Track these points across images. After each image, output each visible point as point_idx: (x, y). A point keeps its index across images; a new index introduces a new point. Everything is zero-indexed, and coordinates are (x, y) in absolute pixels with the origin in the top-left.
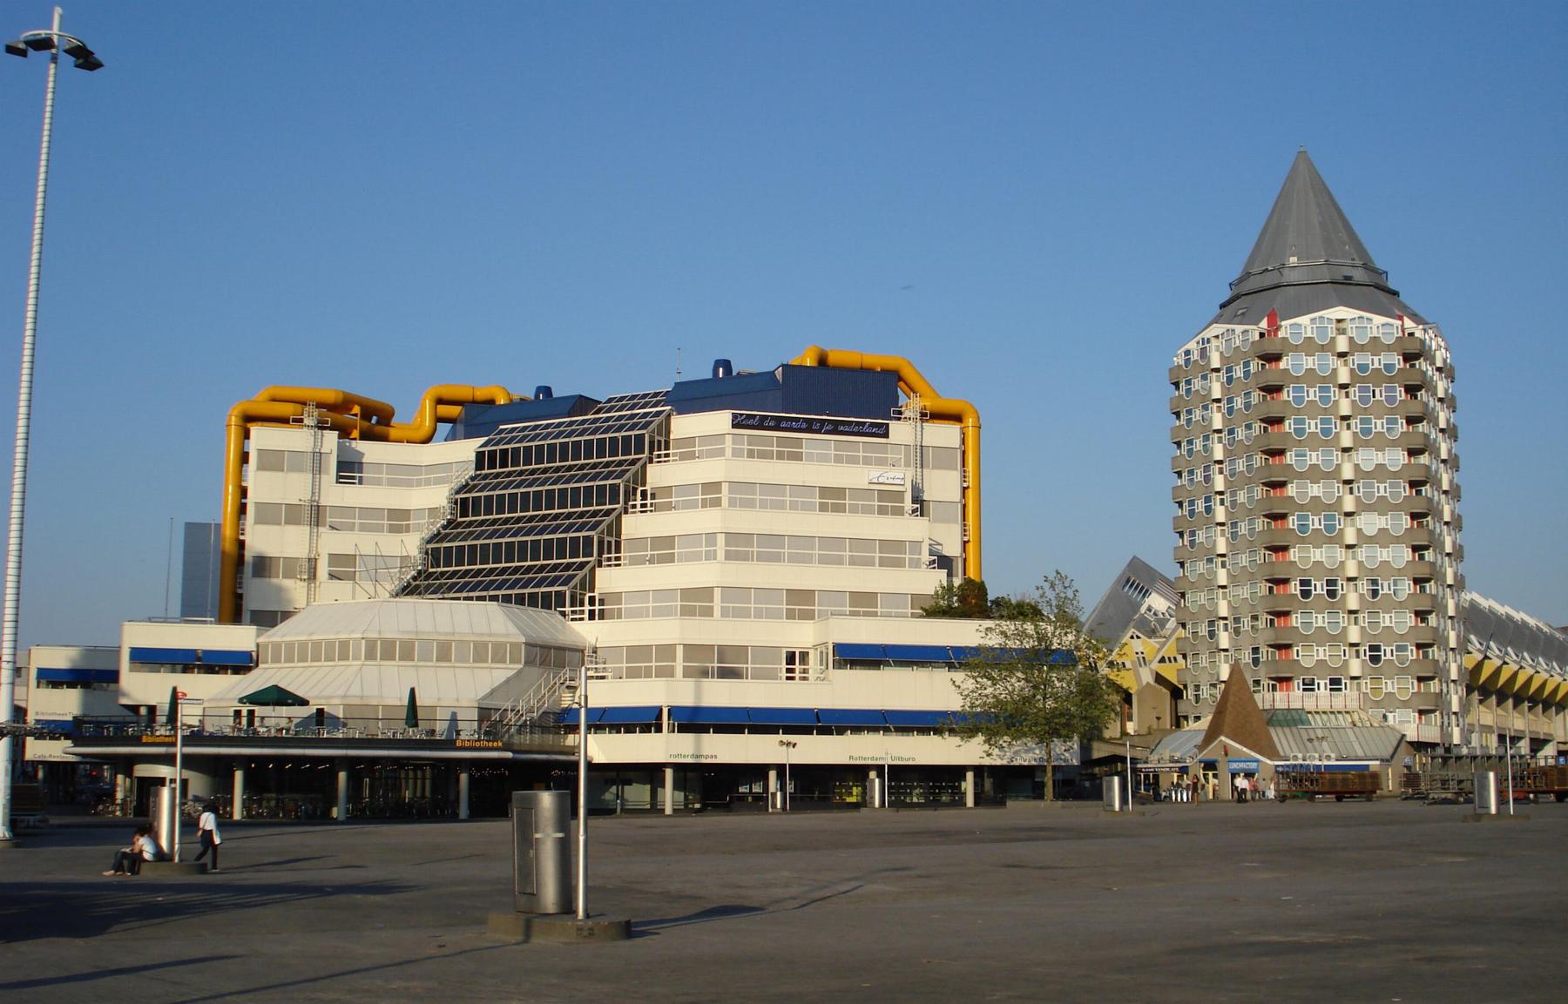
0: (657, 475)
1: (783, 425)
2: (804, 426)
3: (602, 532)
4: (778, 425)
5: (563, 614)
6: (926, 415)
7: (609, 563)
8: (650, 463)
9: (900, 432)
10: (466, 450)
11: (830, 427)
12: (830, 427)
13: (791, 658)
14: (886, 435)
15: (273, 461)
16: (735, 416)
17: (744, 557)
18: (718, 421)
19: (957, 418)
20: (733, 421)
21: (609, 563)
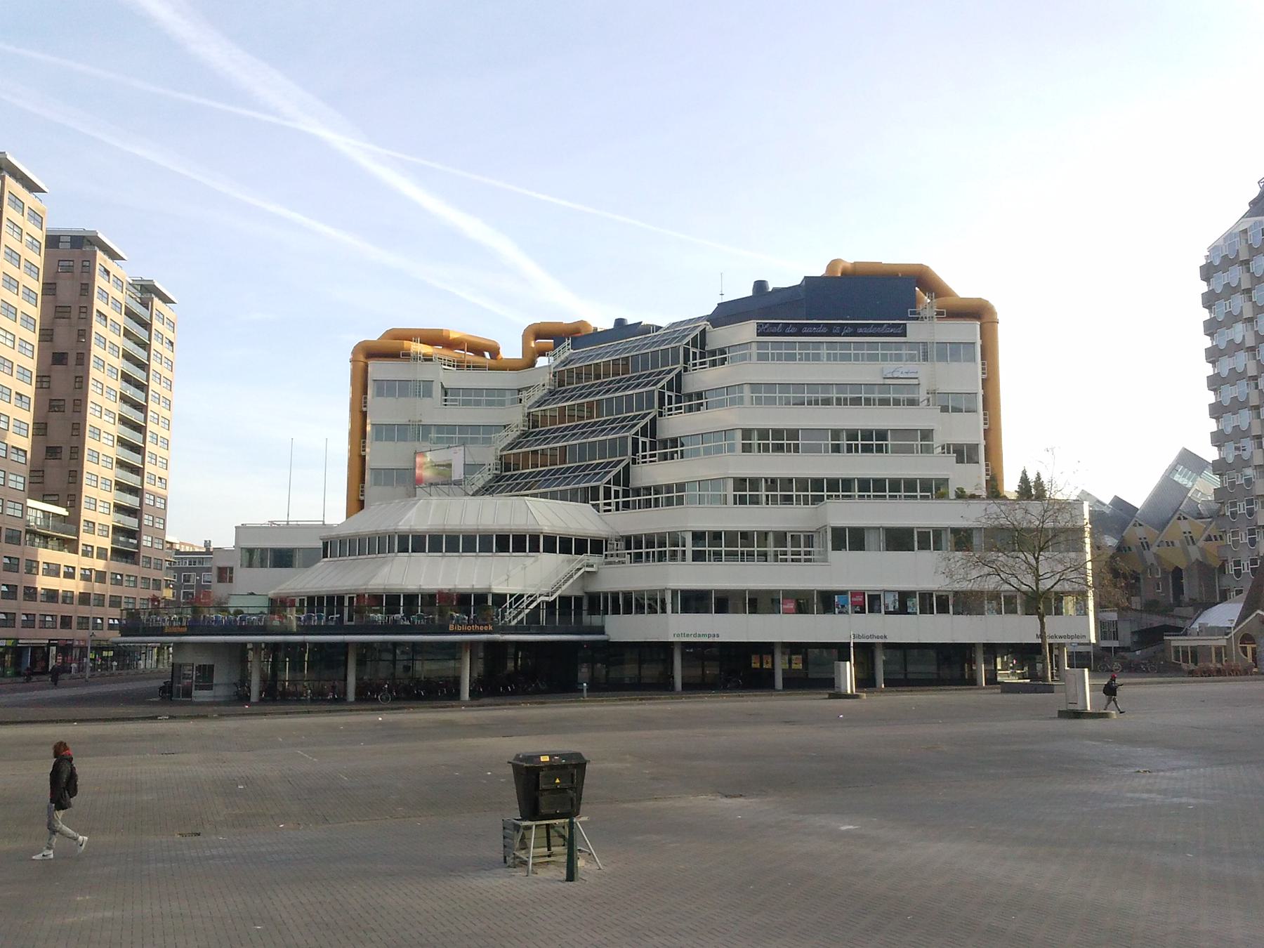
1: (805, 330)
2: (825, 330)
3: (637, 434)
4: (799, 331)
5: (596, 507)
6: (942, 313)
7: (645, 460)
8: (684, 372)
9: (916, 331)
11: (850, 330)
12: (850, 330)
14: (904, 334)
16: (759, 325)
18: (746, 331)
20: (758, 329)
21: (645, 460)
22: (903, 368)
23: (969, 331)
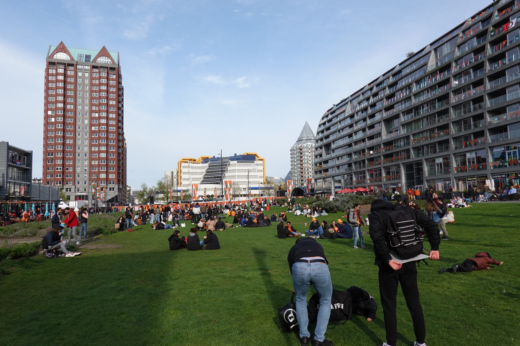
0: (229, 168)
9: (255, 162)
10: (207, 165)
13: (244, 189)
15: (184, 167)
17: (239, 178)
18: (236, 162)
19: (262, 160)
22: (255, 167)
23: (261, 162)
